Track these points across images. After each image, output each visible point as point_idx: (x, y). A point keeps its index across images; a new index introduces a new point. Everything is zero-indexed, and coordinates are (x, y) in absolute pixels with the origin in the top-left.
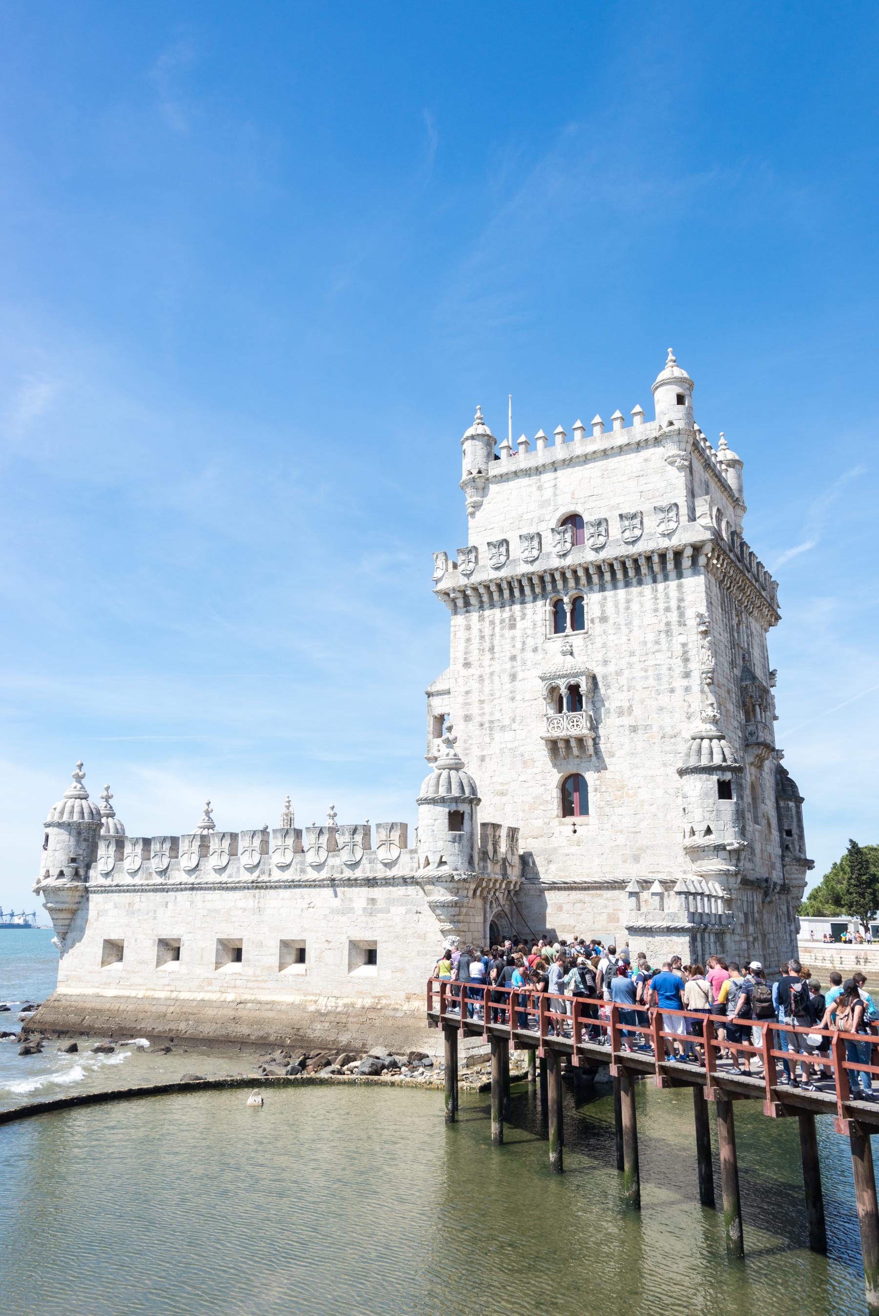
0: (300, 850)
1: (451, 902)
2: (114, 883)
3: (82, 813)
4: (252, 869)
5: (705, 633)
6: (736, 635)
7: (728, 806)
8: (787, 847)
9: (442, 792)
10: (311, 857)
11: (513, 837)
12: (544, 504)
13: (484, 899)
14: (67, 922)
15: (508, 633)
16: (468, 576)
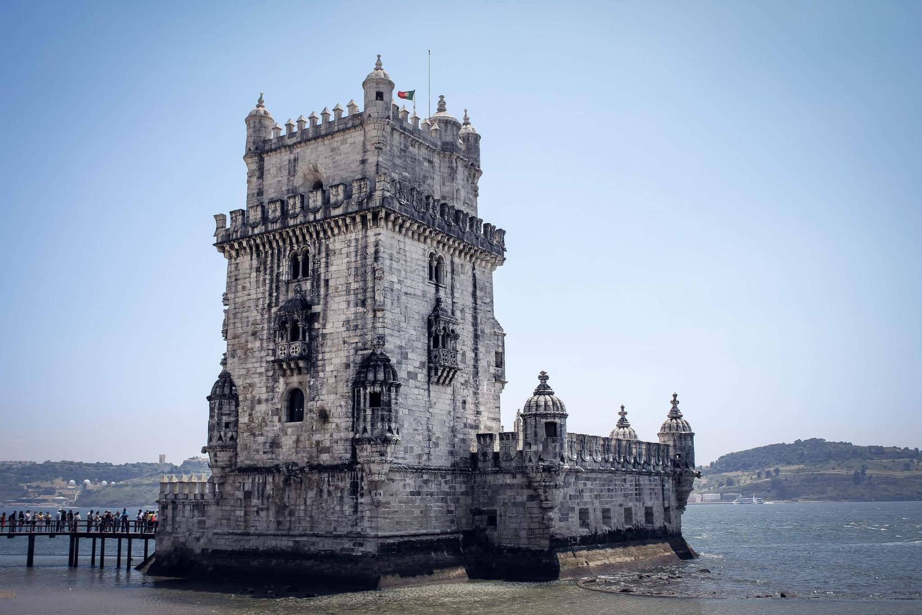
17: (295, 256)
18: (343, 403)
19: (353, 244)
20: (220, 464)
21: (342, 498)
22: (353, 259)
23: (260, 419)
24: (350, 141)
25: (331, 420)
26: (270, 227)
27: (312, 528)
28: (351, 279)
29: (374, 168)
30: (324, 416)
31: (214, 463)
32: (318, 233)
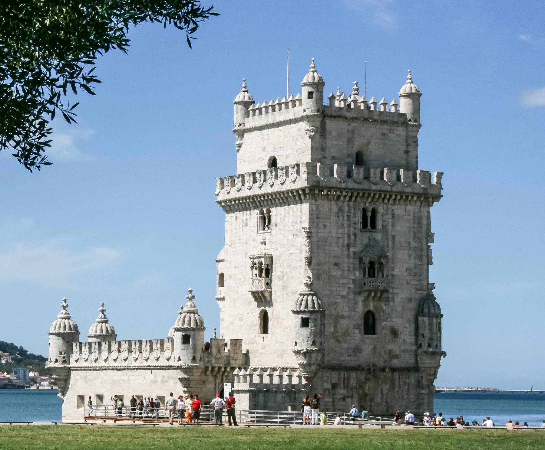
0: (141, 351)
1: (182, 378)
2: (79, 366)
3: (65, 327)
4: (126, 360)
5: (308, 237)
6: (359, 226)
7: (306, 331)
8: (421, 345)
9: (180, 326)
10: (145, 355)
11: (236, 345)
12: (264, 149)
13: (215, 377)
14: (63, 386)
15: (245, 228)
16: (228, 193)
17: (364, 210)
18: (408, 325)
19: (412, 214)
20: (319, 362)
21: (408, 389)
22: (412, 225)
23: (344, 330)
24: (396, 132)
25: (399, 336)
26: (356, 186)
27: (387, 410)
28: (411, 240)
29: (415, 160)
30: (394, 333)
31: (315, 362)
32: (389, 200)
